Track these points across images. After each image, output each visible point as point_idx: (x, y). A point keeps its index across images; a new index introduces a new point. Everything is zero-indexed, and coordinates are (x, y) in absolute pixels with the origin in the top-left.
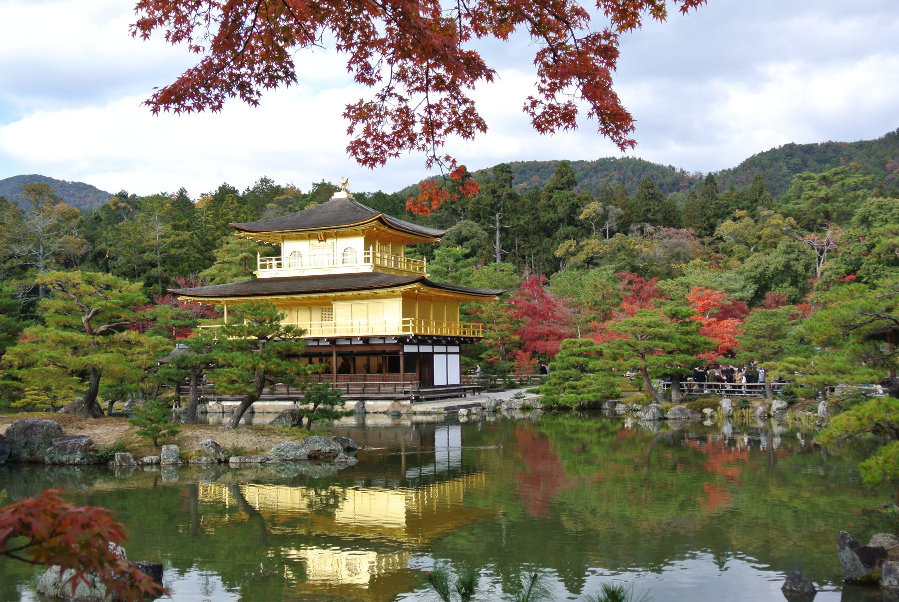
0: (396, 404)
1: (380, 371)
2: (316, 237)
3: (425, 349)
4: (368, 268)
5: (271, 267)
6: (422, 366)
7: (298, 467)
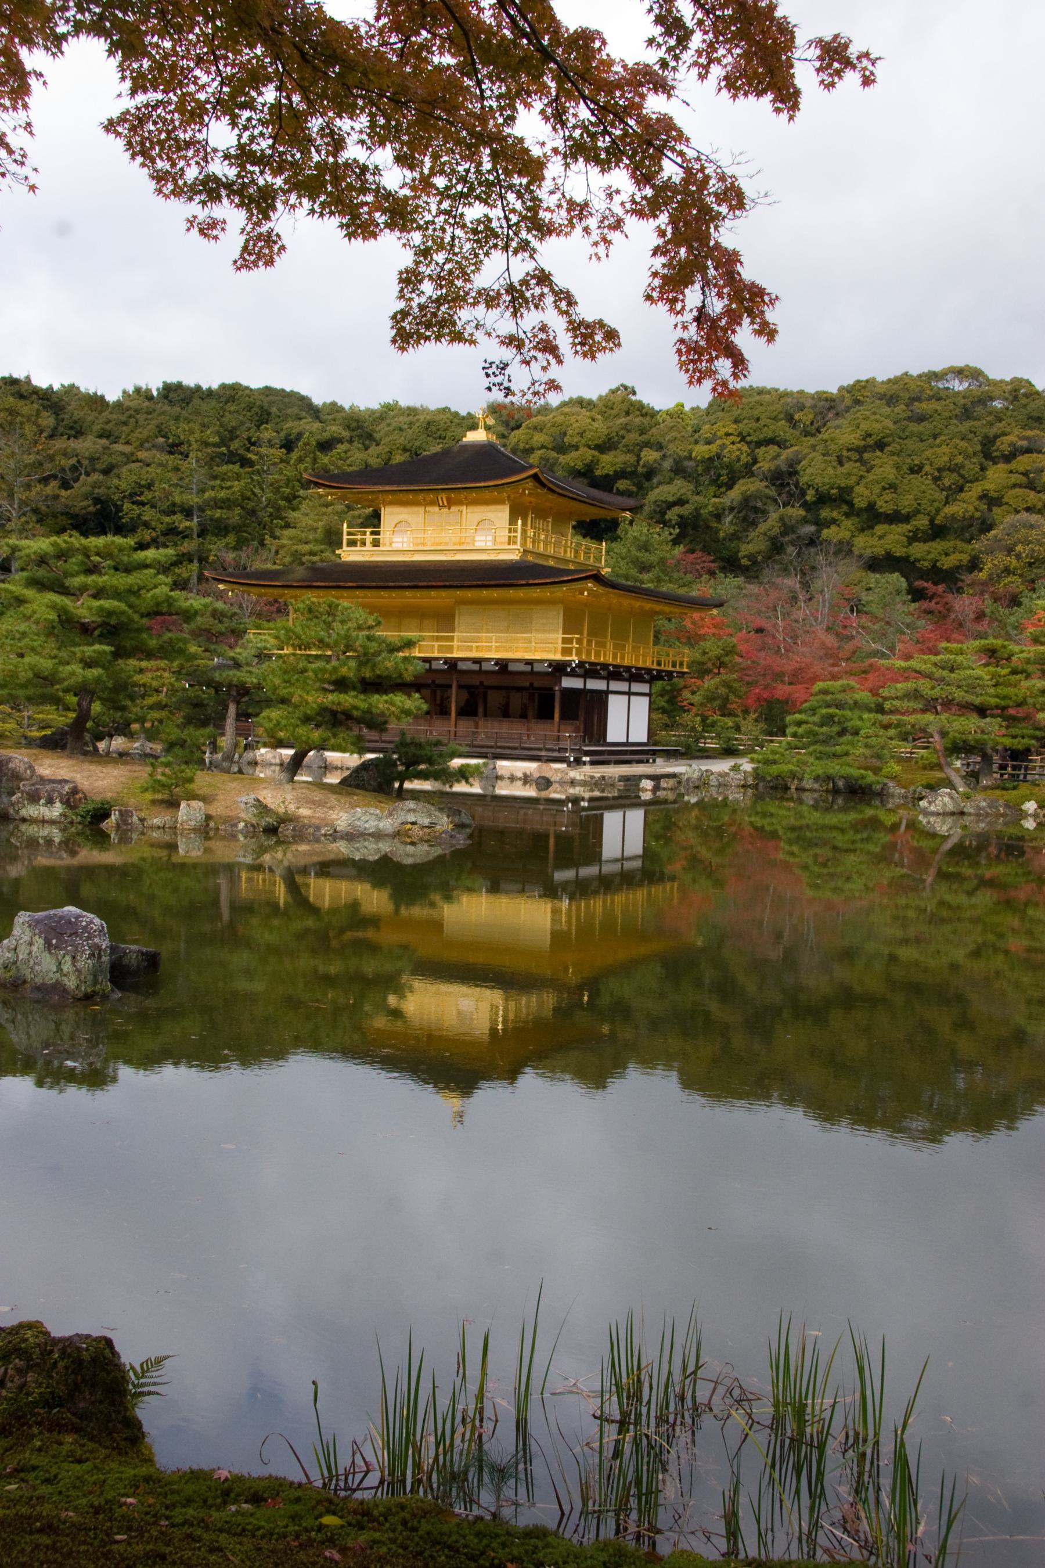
0: (544, 766)
1: (523, 716)
2: (433, 503)
3: (595, 685)
4: (513, 556)
5: (364, 544)
6: (588, 713)
7: (380, 845)
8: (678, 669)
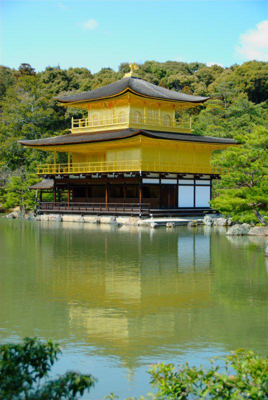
0: (132, 218)
3: (164, 181)
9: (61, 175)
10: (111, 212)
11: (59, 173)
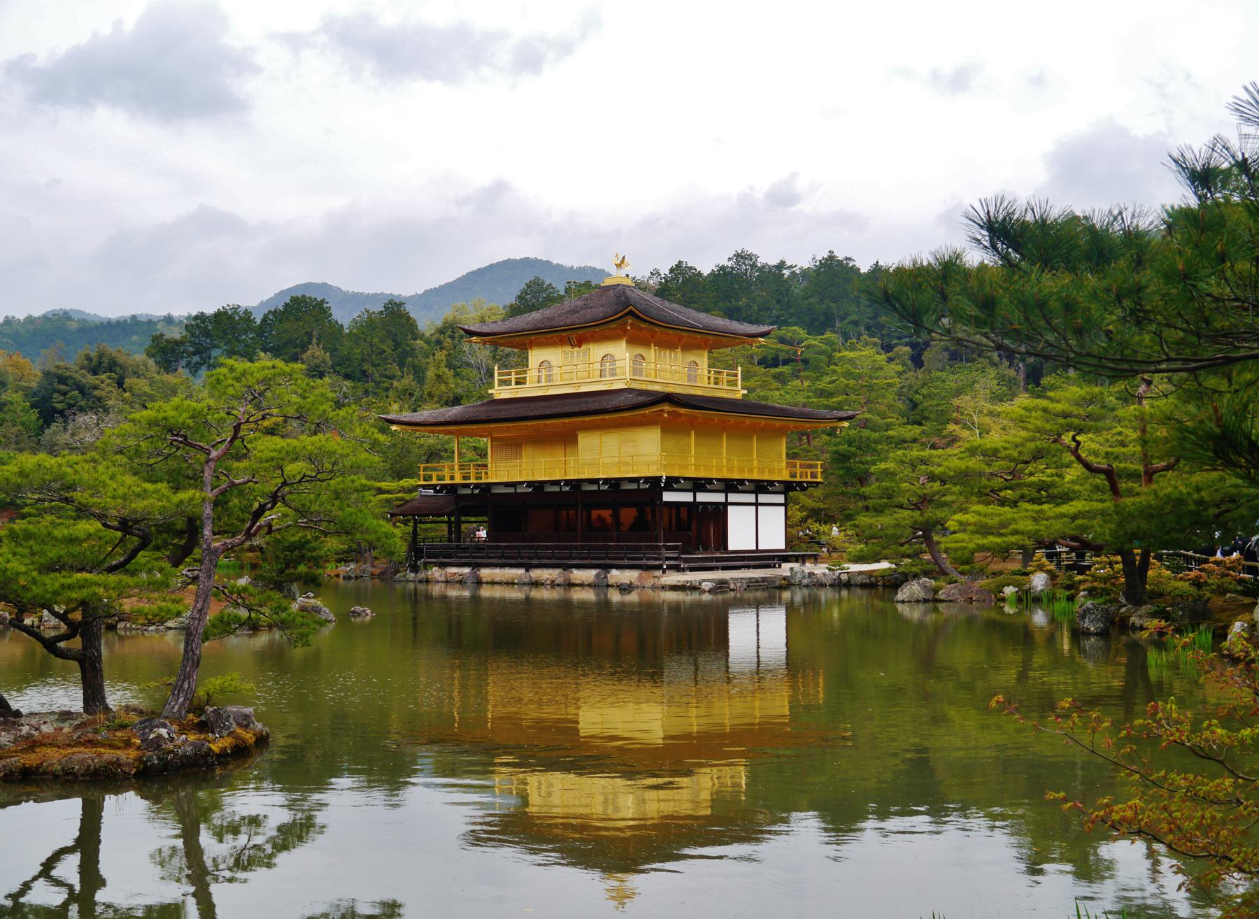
0: (644, 574)
3: (703, 497)
8: (809, 479)
9: (476, 486)
10: (594, 562)
11: (472, 481)
